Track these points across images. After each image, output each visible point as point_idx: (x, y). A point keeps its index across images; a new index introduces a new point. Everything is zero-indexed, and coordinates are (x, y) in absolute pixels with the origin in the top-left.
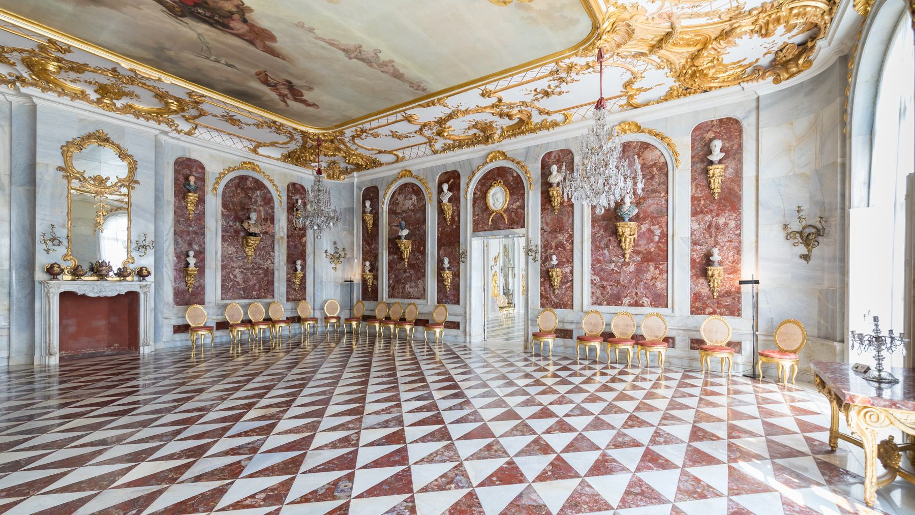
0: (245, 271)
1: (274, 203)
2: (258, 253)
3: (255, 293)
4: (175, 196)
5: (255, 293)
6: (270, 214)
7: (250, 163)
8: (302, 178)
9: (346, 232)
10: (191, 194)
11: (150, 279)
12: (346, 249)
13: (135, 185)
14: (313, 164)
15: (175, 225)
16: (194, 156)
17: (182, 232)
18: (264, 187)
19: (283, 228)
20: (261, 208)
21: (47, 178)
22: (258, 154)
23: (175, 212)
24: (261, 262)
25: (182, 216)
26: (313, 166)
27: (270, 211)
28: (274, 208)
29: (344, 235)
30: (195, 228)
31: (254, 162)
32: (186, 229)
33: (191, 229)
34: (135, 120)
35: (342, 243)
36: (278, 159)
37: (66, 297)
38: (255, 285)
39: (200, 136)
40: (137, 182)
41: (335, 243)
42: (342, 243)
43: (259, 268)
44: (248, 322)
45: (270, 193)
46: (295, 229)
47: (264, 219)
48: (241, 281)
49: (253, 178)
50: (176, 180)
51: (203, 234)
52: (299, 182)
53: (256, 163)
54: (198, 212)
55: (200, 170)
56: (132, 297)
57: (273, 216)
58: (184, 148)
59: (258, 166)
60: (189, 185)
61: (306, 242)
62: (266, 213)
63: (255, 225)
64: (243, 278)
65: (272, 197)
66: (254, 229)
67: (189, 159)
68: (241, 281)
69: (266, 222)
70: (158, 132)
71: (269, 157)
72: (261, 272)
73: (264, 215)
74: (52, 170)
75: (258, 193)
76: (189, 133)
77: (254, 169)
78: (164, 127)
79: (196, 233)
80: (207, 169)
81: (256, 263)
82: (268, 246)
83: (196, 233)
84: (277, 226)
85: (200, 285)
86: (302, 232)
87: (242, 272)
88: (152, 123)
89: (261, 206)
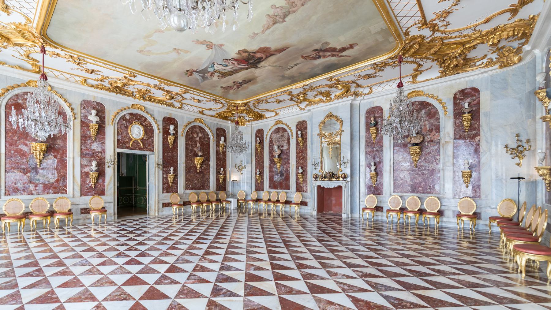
0: (412, 173)
1: (439, 115)
2: (423, 158)
3: (421, 189)
4: (366, 132)
5: (421, 189)
6: (435, 125)
7: (413, 92)
8: (472, 81)
9: (530, 120)
10: (371, 129)
11: (349, 179)
12: (531, 141)
13: (343, 133)
14: (478, 63)
15: (366, 148)
16: (375, 105)
17: (370, 152)
18: (429, 104)
19: (449, 134)
20: (426, 122)
21: (315, 140)
22: (416, 83)
23: (366, 141)
24: (427, 164)
25: (370, 142)
26: (480, 65)
27: (435, 123)
28: (439, 119)
29: (528, 123)
30: (377, 148)
31: (416, 90)
32: (372, 150)
33: (375, 149)
34: (338, 101)
35: (527, 134)
36: (440, 77)
37: (319, 187)
38: (420, 183)
39: (377, 91)
40: (343, 131)
41: (518, 135)
42: (527, 134)
43: (425, 169)
44: (421, 212)
45: (435, 107)
46: (464, 132)
47: (429, 131)
48: (408, 180)
49: (418, 102)
50: (367, 122)
51: (382, 151)
52: (469, 86)
53: (419, 89)
54: (378, 138)
55: (380, 112)
56: (340, 188)
57: (439, 126)
58: (370, 103)
59: (420, 91)
60: (371, 123)
61: (479, 141)
62: (431, 125)
63: (416, 137)
64: (410, 178)
65: (437, 110)
66: (414, 140)
67: (373, 108)
68: (408, 180)
69: (432, 132)
70: (350, 102)
71: (427, 80)
72: (426, 172)
73: (430, 127)
74: (316, 135)
75: (424, 111)
76: (369, 93)
77: (417, 95)
78: (351, 98)
79: (377, 151)
80: (384, 109)
81: (422, 166)
82: (433, 151)
83: (377, 151)
84: (442, 133)
85: (380, 183)
86: (474, 132)
87: (409, 173)
88: (345, 99)
89: (426, 121)
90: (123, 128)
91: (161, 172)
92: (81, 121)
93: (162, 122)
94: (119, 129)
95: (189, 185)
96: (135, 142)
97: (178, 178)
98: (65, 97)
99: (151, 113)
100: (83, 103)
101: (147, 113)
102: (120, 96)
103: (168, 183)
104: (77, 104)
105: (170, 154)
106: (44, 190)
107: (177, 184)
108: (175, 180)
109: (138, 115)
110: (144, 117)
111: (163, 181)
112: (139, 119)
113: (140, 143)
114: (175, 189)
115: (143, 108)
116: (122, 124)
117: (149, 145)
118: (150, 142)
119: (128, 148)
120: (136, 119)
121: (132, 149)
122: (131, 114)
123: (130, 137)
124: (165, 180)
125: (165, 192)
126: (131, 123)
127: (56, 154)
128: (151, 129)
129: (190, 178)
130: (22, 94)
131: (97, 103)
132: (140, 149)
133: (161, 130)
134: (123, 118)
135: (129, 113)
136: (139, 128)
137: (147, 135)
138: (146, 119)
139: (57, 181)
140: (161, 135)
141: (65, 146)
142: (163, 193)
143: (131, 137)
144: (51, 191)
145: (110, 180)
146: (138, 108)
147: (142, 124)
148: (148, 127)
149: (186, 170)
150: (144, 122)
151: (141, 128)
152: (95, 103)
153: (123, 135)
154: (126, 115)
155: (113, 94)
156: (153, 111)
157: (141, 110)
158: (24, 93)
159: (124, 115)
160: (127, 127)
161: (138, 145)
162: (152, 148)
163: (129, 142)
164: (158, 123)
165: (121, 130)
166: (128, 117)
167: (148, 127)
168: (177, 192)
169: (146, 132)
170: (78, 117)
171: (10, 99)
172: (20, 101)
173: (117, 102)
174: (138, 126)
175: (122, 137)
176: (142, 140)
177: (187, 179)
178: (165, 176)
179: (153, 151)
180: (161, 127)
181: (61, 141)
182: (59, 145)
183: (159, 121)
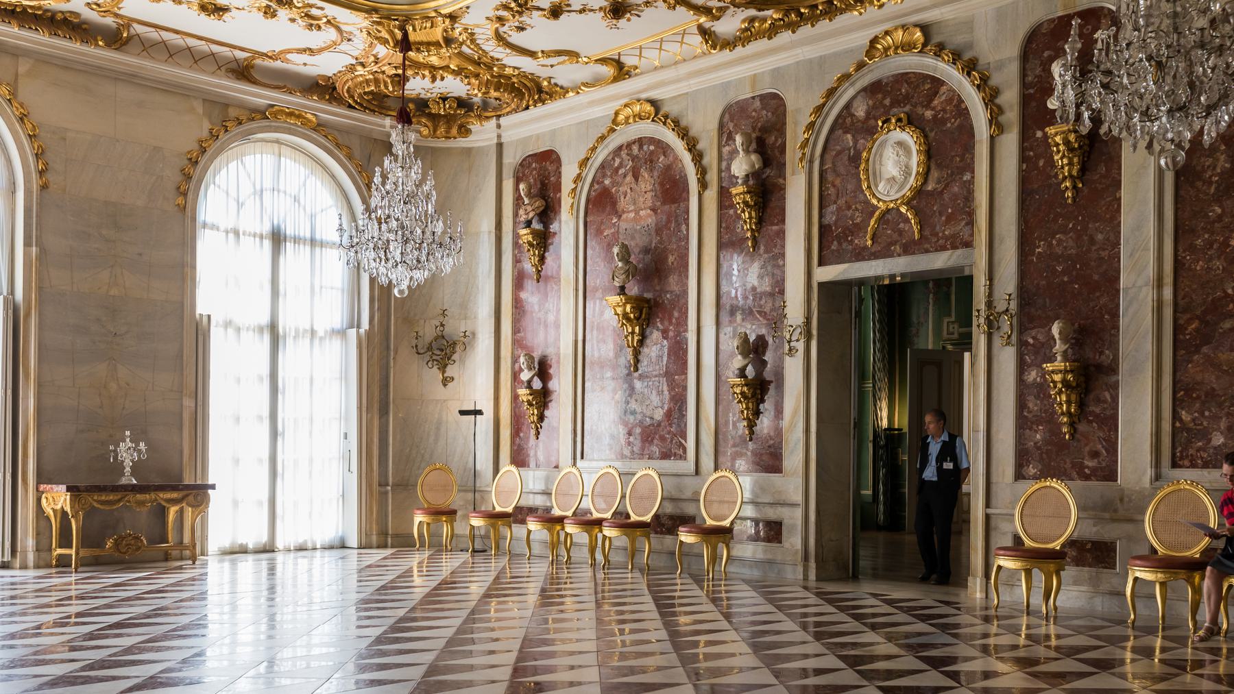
90: (842, 170)
91: (1007, 358)
92: (722, 187)
93: (1013, 70)
94: (830, 177)
95: (1205, 435)
96: (889, 217)
97: (1115, 387)
98: (683, 123)
99: (958, 40)
100: (727, 116)
101: (940, 50)
102: (806, 30)
103: (1050, 419)
104: (705, 125)
105: (1064, 243)
106: (643, 449)
107: (1110, 422)
108: (1099, 401)
109: (903, 78)
110: (926, 77)
111: (1021, 405)
112: (907, 99)
113: (907, 220)
114: (1095, 455)
115: (918, 34)
116: (839, 153)
117: (950, 219)
118: (955, 197)
119: (860, 255)
120: (896, 103)
121: (875, 256)
122: (874, 89)
123: (867, 202)
124: (1033, 404)
125: (1032, 470)
126: (871, 132)
127: (666, 323)
128: (961, 127)
129: (1211, 379)
130: (610, 158)
131: (763, 98)
132: (907, 250)
133: (1012, 116)
134: (844, 121)
135: (864, 90)
136: (900, 144)
137: (939, 166)
138: (937, 83)
139: (669, 414)
140: (1010, 143)
141: (685, 293)
142: (1019, 476)
143: (874, 202)
144: (655, 449)
145: (795, 412)
146: (897, 48)
147: (911, 121)
148: (943, 121)
149: (1177, 329)
150: (928, 106)
151: (908, 137)
152: (758, 104)
153: (841, 202)
154: (855, 104)
155: (785, 37)
156: (968, 24)
157: (907, 47)
158: (614, 152)
159: (848, 106)
160: (855, 159)
161: (901, 232)
162: (967, 230)
163: (859, 228)
164: (994, 81)
165: (838, 182)
166: (860, 111)
167: (943, 121)
168: (1110, 474)
169: (930, 154)
170: (712, 177)
171: (592, 185)
172: (607, 182)
173: (822, 60)
174: (899, 135)
175: (839, 209)
176: (918, 200)
177: (1183, 393)
178: (1032, 376)
179: (968, 244)
180: (1010, 97)
181: (675, 277)
182: (672, 292)
183: (1001, 65)
